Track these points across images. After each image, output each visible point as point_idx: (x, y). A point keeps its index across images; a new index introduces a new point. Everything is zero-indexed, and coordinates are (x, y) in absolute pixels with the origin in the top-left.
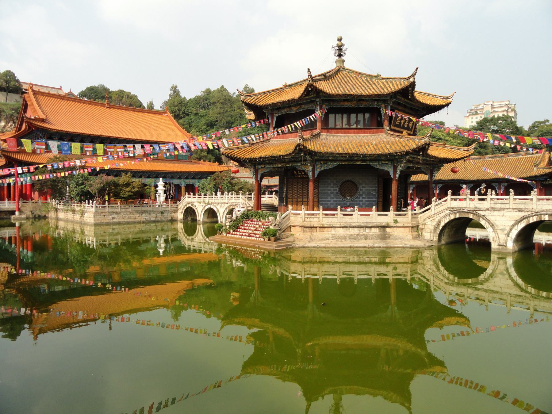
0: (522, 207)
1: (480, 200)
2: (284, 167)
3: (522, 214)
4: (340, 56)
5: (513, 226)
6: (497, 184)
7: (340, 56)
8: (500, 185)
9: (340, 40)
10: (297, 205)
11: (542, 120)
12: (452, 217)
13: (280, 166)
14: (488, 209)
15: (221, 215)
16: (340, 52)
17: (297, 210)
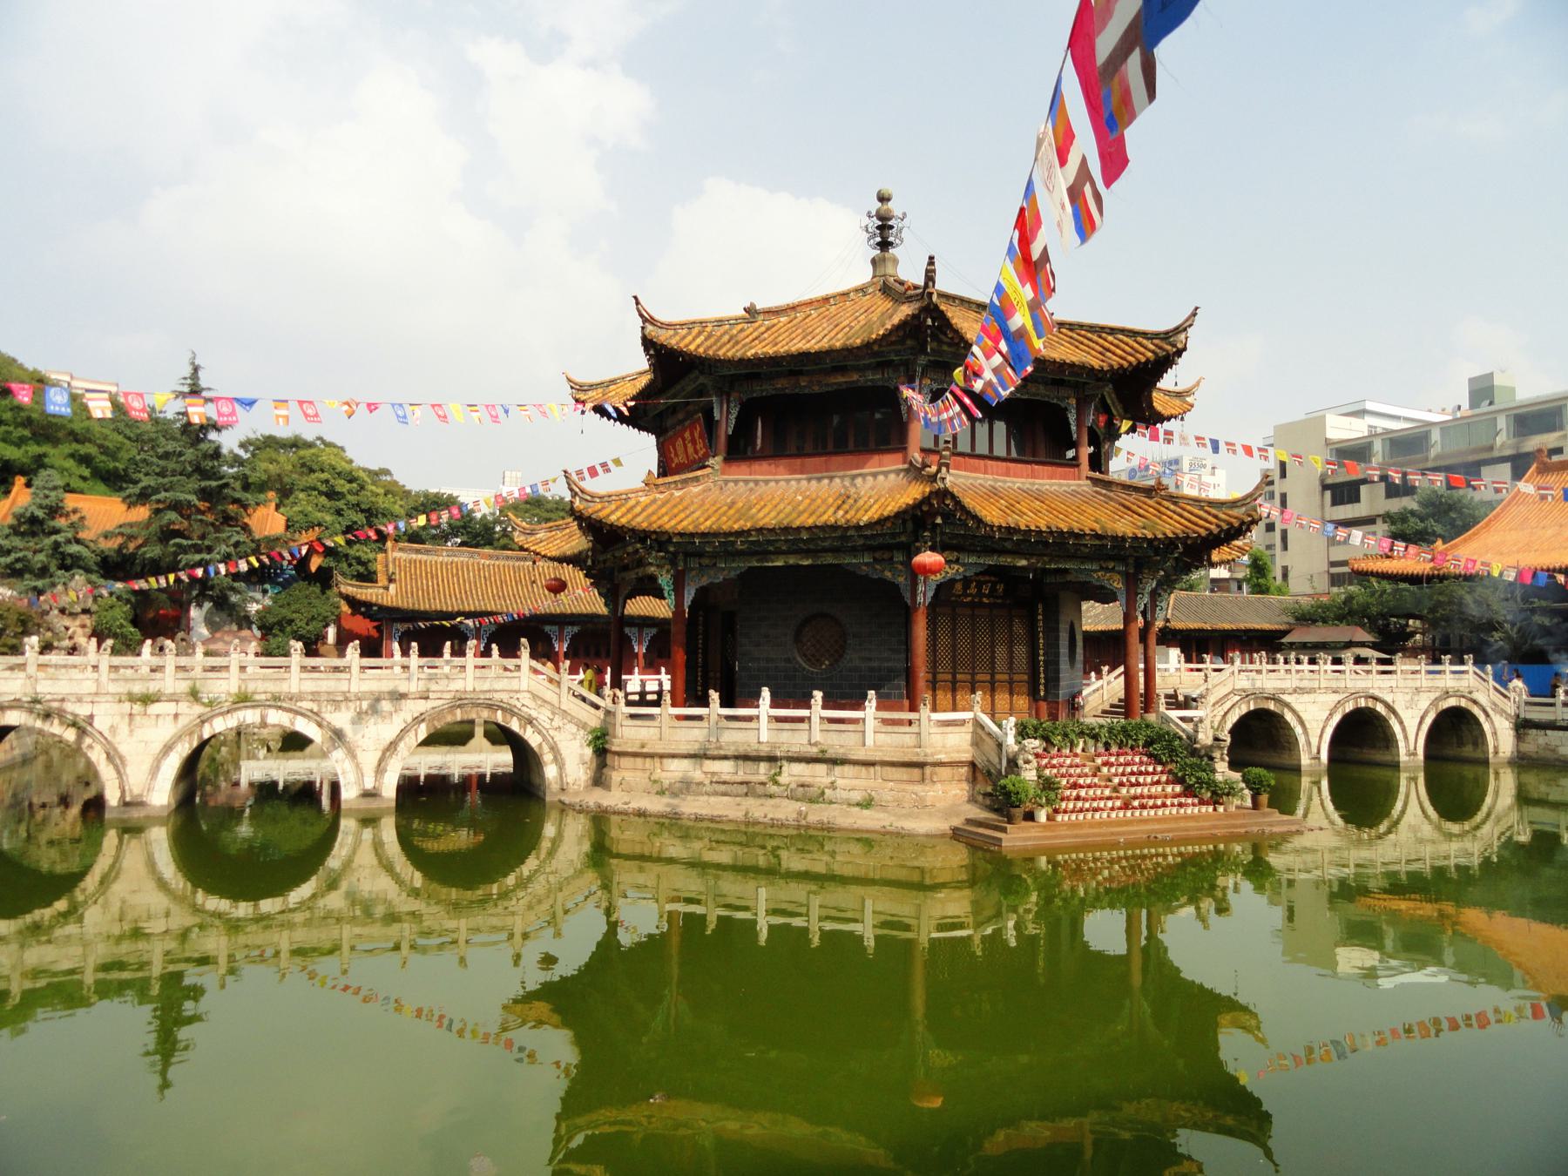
0: (1334, 684)
1: (1430, 672)
2: (1035, 570)
3: (1337, 697)
4: (884, 245)
5: (1328, 719)
6: (556, 628)
7: (884, 245)
8: (640, 635)
10: (954, 690)
11: (375, 467)
12: (1244, 710)
13: (1023, 563)
14: (1295, 691)
15: (369, 759)
16: (884, 234)
17: (954, 709)
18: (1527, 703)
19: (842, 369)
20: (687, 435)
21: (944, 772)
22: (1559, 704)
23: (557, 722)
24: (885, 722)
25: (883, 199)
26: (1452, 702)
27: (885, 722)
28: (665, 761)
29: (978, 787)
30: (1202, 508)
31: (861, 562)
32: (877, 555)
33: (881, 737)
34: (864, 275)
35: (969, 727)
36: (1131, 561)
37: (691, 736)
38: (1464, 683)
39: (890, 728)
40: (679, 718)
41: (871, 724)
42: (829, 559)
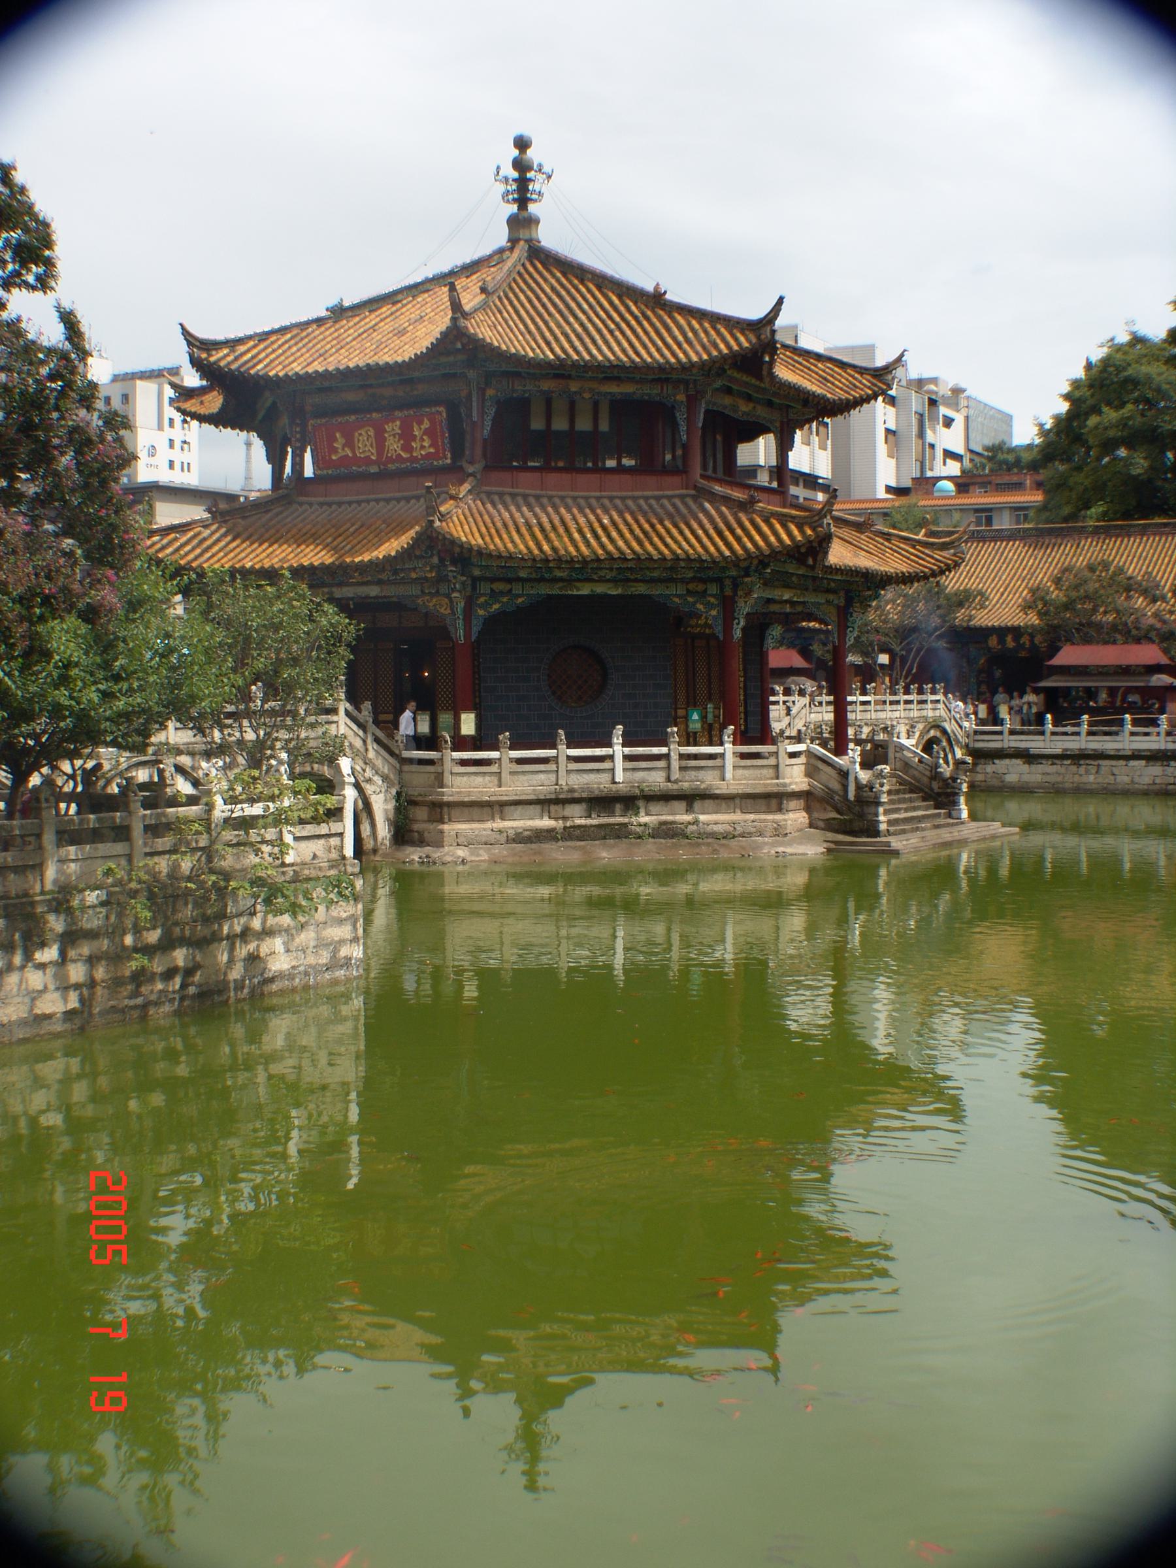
4: (523, 201)
7: (523, 201)
9: (522, 144)
18: (976, 732)
19: (618, 379)
20: (394, 427)
21: (793, 804)
22: (1006, 732)
23: (369, 773)
24: (743, 756)
25: (522, 144)
26: (932, 733)
27: (743, 756)
28: (507, 808)
29: (815, 815)
30: (914, 547)
31: (674, 594)
32: (691, 586)
33: (740, 772)
34: (500, 236)
35: (802, 759)
36: (842, 594)
37: (537, 783)
38: (937, 713)
39: (748, 762)
40: (520, 761)
41: (730, 760)
42: (642, 589)
